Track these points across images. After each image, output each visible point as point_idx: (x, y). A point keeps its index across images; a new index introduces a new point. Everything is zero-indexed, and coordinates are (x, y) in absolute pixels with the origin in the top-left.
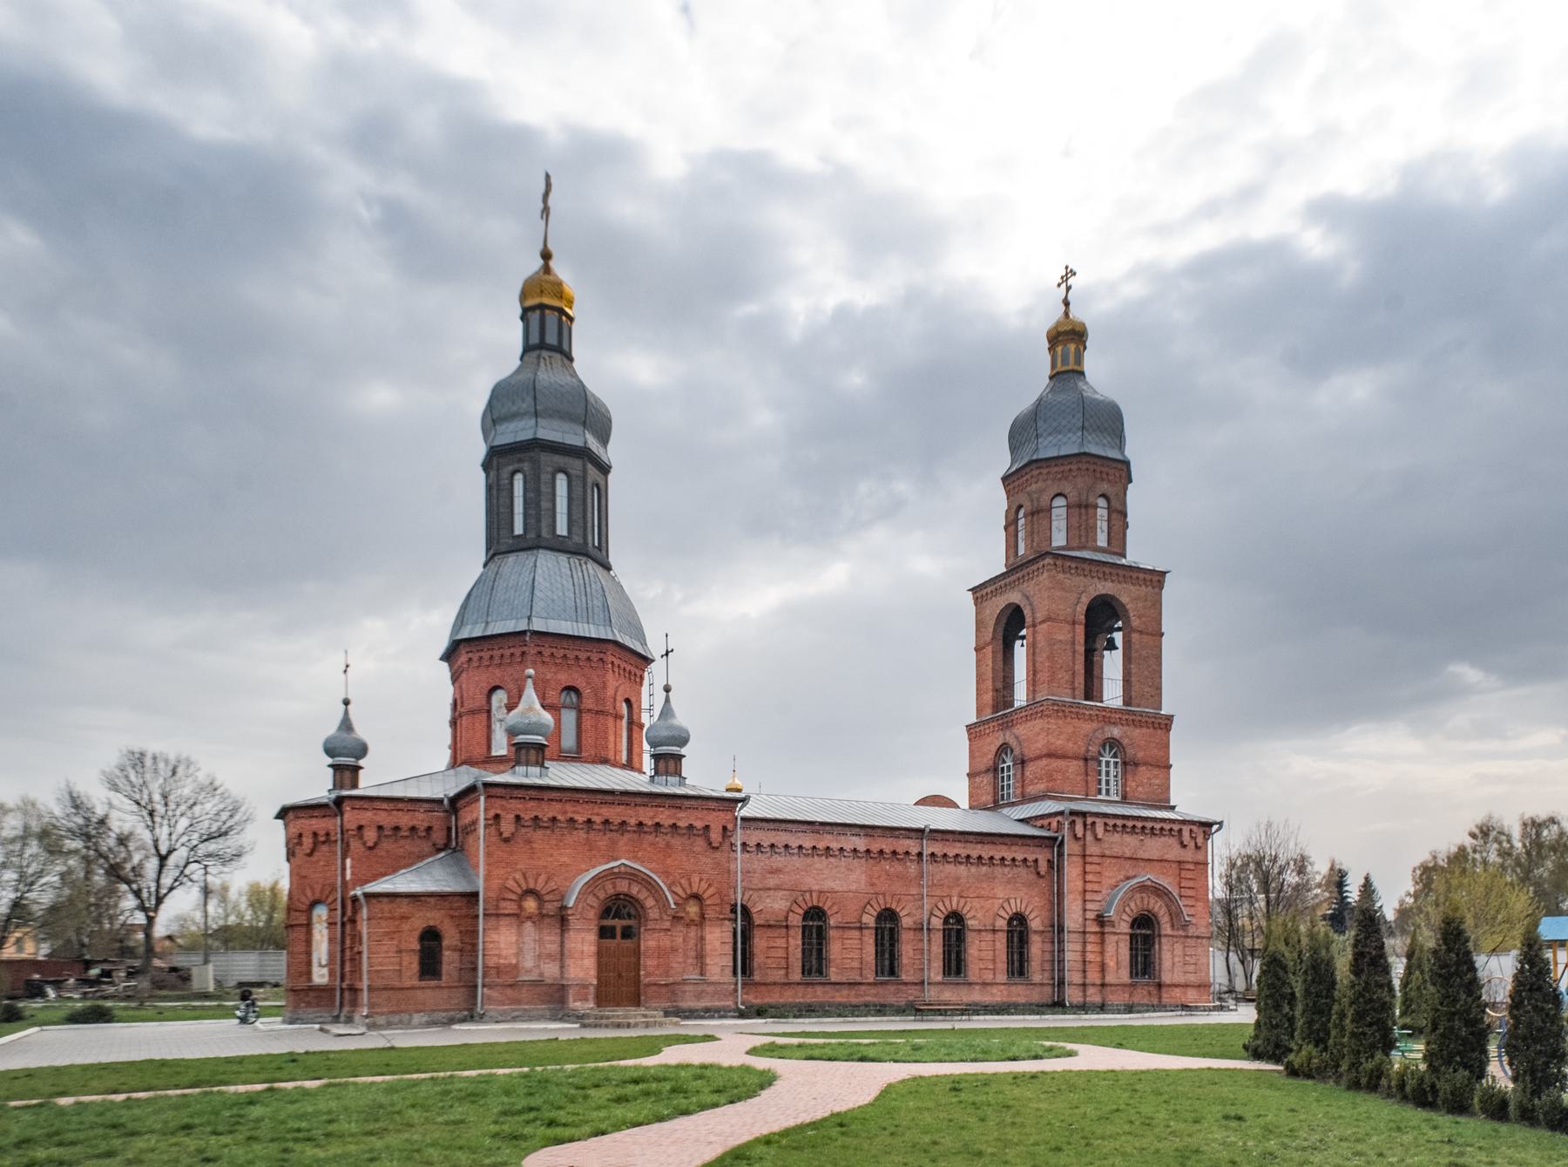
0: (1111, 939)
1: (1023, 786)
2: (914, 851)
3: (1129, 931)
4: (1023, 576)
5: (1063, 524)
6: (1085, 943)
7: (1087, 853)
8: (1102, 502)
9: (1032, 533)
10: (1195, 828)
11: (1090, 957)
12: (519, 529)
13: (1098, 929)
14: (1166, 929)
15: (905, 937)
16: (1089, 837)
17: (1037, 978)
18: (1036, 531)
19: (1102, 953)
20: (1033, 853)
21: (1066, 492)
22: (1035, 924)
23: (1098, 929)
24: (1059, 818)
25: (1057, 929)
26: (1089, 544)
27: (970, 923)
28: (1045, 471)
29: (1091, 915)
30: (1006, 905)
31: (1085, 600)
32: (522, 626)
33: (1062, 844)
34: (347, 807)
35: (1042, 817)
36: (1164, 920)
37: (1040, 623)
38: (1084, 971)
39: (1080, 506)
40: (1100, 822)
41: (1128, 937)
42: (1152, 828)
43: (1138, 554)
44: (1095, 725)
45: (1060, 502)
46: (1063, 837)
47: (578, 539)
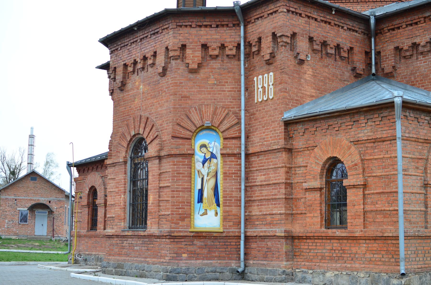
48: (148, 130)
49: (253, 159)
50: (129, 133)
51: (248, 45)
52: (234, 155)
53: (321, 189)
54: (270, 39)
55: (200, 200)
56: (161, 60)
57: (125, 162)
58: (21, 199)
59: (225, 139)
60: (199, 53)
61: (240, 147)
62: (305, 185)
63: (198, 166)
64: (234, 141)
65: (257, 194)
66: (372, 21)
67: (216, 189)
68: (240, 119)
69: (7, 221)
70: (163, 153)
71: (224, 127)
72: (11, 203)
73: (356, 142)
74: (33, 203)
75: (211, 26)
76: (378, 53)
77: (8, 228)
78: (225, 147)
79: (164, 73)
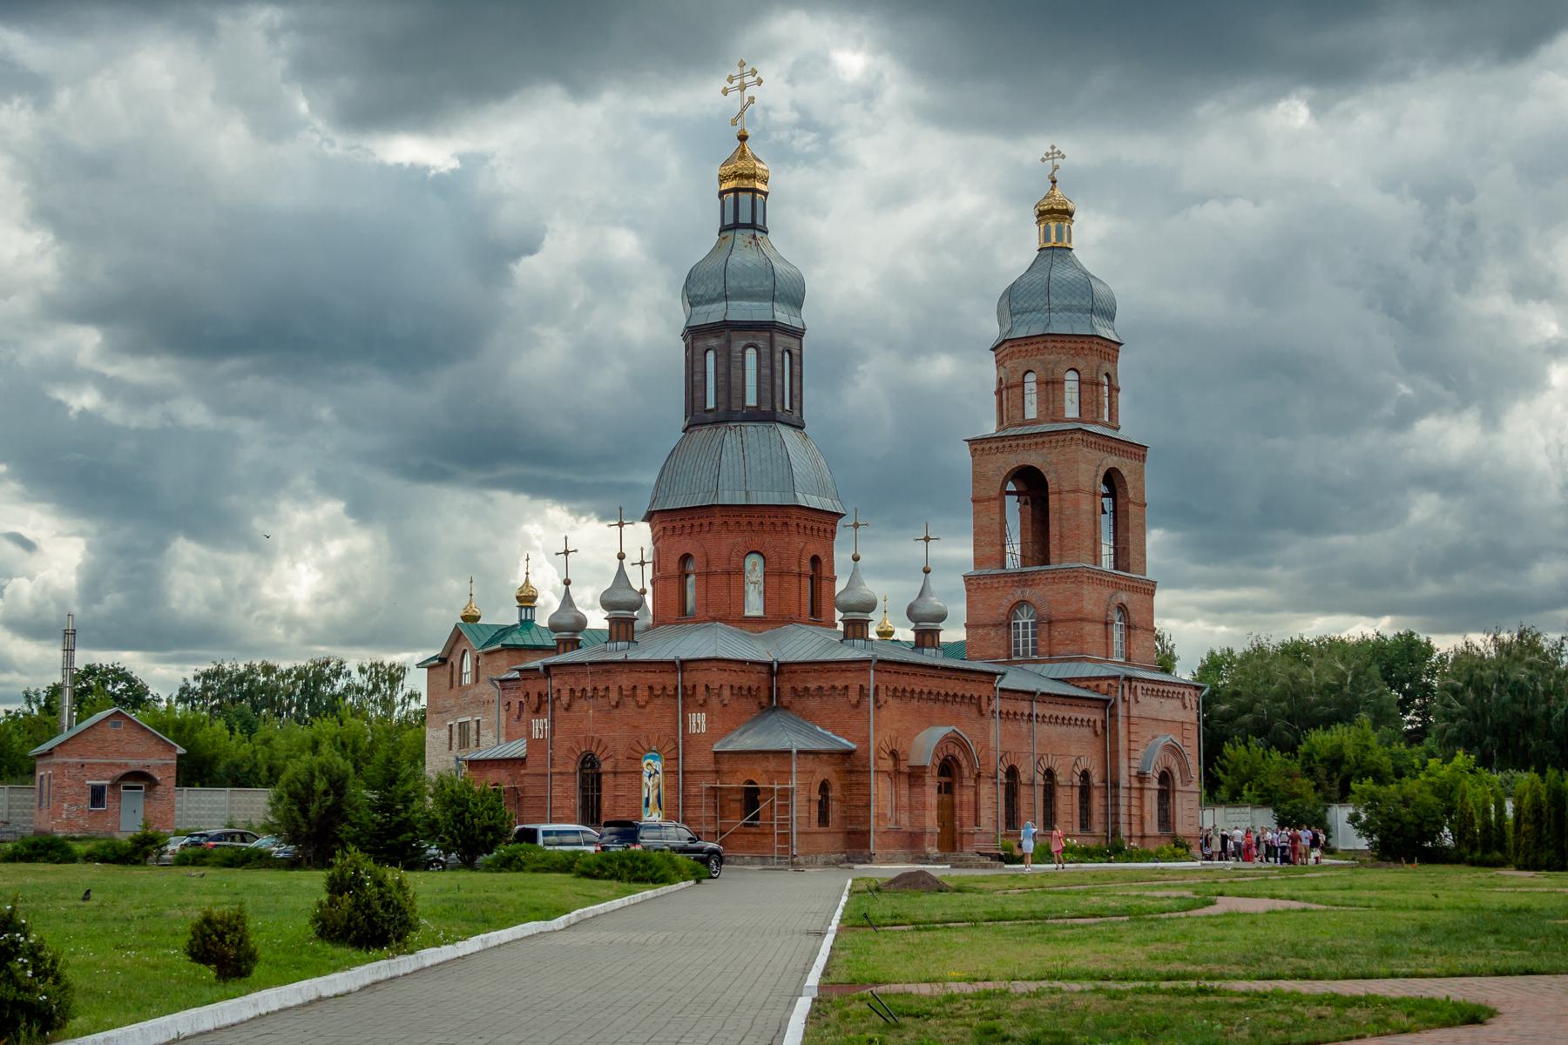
0: (1147, 794)
1: (1050, 644)
2: (1027, 712)
3: (1158, 787)
4: (1043, 442)
5: (1075, 397)
6: (1130, 798)
7: (1132, 714)
8: (1105, 380)
9: (1048, 401)
10: (1192, 692)
11: (1134, 811)
12: (751, 400)
13: (1138, 785)
14: (1179, 786)
15: (1023, 791)
16: (1132, 700)
17: (1098, 829)
18: (1051, 399)
19: (1141, 807)
20: (1094, 714)
22: (1096, 780)
23: (1138, 785)
24: (1110, 682)
26: (1100, 420)
27: (1059, 779)
28: (1059, 345)
29: (1134, 772)
30: (1078, 762)
31: (1102, 473)
32: (788, 500)
33: (1114, 706)
34: (553, 671)
35: (1088, 679)
36: (1177, 776)
37: (1067, 492)
38: (1130, 824)
39: (1092, 384)
40: (1139, 685)
42: (1169, 692)
43: (1129, 428)
45: (1071, 376)
46: (1115, 699)
47: (766, 408)
48: (601, 749)
49: (687, 775)
50: (579, 749)
51: (684, 688)
52: (673, 772)
53: (740, 800)
54: (703, 688)
55: (647, 805)
56: (614, 696)
57: (575, 773)
58: (92, 764)
59: (666, 759)
60: (647, 693)
61: (678, 766)
62: (730, 797)
63: (645, 779)
64: (673, 762)
65: (691, 802)
66: (775, 666)
67: (659, 794)
68: (677, 744)
69: (65, 805)
70: (619, 770)
71: (666, 751)
72: (73, 771)
73: (766, 772)
74: (123, 771)
75: (655, 672)
76: (778, 689)
77: (68, 818)
79: (617, 705)
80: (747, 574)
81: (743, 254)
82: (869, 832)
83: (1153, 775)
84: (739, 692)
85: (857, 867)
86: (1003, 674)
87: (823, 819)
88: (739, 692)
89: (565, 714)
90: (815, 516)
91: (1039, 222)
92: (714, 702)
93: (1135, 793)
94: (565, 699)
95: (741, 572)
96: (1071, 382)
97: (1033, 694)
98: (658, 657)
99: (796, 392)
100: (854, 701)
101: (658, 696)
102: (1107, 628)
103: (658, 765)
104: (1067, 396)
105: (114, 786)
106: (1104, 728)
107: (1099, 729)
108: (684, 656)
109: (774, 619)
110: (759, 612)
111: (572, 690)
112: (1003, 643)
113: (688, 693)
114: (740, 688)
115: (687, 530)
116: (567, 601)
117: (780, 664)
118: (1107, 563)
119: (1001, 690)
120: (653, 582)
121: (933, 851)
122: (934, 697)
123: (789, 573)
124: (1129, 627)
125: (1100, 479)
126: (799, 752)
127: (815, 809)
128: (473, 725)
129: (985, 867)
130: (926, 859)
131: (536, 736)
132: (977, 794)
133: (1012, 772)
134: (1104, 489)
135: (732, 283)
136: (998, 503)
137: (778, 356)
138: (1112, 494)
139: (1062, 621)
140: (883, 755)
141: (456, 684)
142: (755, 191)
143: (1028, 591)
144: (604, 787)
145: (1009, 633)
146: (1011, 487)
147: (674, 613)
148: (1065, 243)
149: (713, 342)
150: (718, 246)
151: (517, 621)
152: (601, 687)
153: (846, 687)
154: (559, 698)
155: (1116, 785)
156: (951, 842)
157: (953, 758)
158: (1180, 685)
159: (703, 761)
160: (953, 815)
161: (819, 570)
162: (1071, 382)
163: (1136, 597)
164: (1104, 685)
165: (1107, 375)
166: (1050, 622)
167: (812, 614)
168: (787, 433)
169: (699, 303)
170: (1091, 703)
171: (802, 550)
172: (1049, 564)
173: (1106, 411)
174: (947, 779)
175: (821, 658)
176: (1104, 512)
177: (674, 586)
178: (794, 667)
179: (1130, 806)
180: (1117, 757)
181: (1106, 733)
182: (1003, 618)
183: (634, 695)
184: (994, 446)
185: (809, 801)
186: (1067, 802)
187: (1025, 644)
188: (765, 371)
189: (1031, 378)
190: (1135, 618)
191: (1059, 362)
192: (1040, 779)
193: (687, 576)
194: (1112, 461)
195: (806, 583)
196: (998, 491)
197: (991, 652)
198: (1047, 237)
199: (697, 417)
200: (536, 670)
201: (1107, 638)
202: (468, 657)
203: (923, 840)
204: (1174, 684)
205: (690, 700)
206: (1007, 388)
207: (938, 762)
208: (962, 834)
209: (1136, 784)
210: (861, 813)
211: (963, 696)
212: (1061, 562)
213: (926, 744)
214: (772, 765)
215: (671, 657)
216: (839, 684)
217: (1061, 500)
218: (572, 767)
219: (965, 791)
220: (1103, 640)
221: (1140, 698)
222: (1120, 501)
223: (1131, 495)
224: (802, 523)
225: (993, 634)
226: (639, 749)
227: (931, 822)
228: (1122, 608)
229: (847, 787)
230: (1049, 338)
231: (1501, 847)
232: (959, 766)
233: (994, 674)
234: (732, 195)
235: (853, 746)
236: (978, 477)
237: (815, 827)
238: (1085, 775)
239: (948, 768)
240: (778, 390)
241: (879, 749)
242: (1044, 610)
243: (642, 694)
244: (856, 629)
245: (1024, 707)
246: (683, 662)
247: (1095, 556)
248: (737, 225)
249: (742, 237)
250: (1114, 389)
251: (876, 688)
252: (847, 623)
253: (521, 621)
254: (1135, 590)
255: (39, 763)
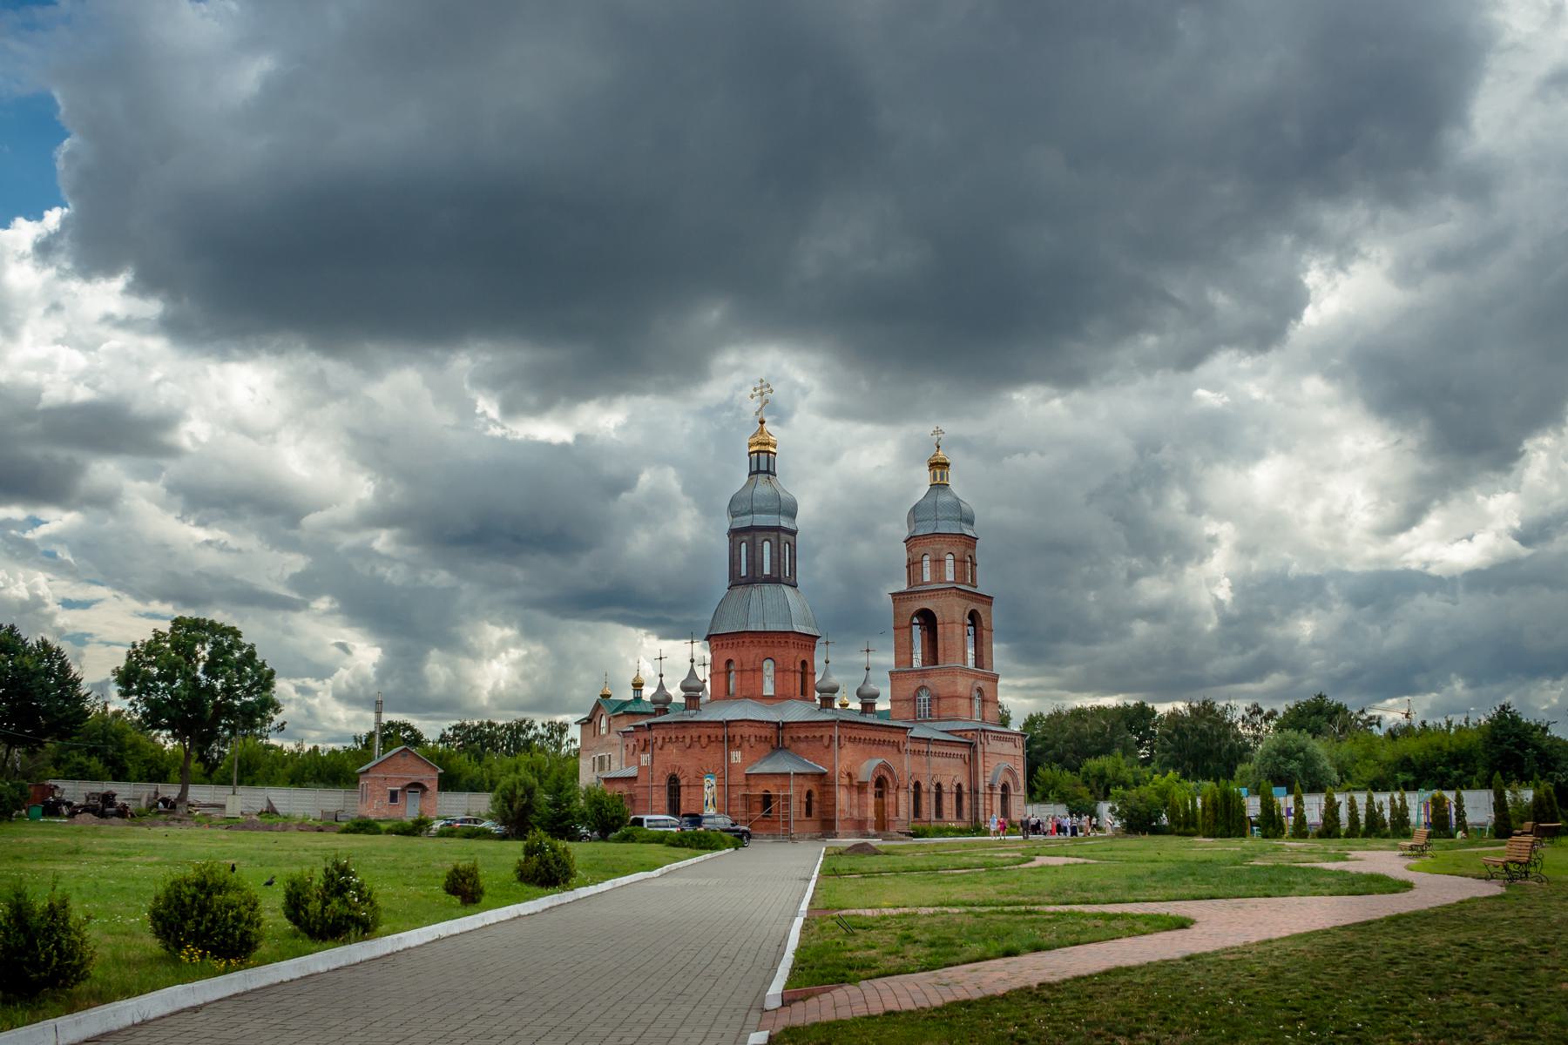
0: (994, 796)
2: (925, 750)
3: (1000, 792)
6: (985, 799)
8: (969, 559)
10: (1020, 737)
11: (987, 807)
12: (767, 571)
14: (1013, 792)
15: (924, 796)
17: (966, 817)
19: (991, 805)
21: (954, 550)
22: (965, 789)
24: (974, 732)
25: (974, 791)
28: (942, 539)
29: (987, 784)
31: (967, 613)
33: (976, 746)
35: (961, 731)
38: (985, 814)
39: (961, 561)
40: (990, 734)
41: (1000, 796)
44: (973, 680)
45: (951, 557)
51: (728, 737)
53: (760, 802)
55: (707, 804)
56: (688, 741)
60: (706, 740)
63: (706, 790)
65: (732, 802)
66: (781, 724)
67: (713, 799)
69: (376, 802)
73: (776, 785)
74: (409, 782)
76: (782, 738)
78: (718, 782)
79: (689, 747)
80: (765, 671)
81: (763, 487)
82: (835, 820)
83: (998, 786)
84: (759, 739)
85: (828, 840)
86: (912, 728)
87: (809, 813)
88: (759, 739)
89: (660, 752)
90: (803, 637)
91: (930, 470)
92: (746, 745)
93: (987, 797)
94: (660, 742)
95: (761, 670)
96: (949, 561)
97: (929, 739)
98: (712, 719)
99: (792, 566)
100: (826, 744)
101: (713, 742)
102: (971, 703)
103: (713, 782)
104: (947, 568)
105: (403, 790)
106: (970, 759)
107: (967, 760)
108: (729, 718)
109: (780, 697)
110: (772, 694)
111: (664, 738)
112: (912, 711)
113: (731, 740)
114: (761, 737)
115: (730, 646)
116: (661, 687)
117: (783, 723)
118: (971, 663)
119: (911, 737)
120: (711, 676)
121: (872, 831)
122: (874, 742)
123: (789, 670)
124: (984, 701)
125: (967, 615)
126: (795, 774)
127: (804, 806)
128: (607, 758)
129: (902, 840)
130: (868, 836)
131: (643, 764)
132: (897, 798)
133: (917, 785)
134: (969, 622)
135: (755, 504)
136: (908, 630)
137: (782, 546)
138: (974, 624)
139: (945, 697)
140: (843, 776)
141: (597, 734)
142: (769, 452)
143: (926, 680)
144: (682, 794)
145: (915, 704)
146: (916, 620)
147: (724, 695)
148: (945, 482)
149: (745, 538)
150: (748, 483)
151: (632, 698)
152: (681, 736)
153: (822, 737)
154: (656, 742)
155: (977, 792)
156: (882, 825)
157: (884, 777)
158: (1013, 734)
159: (741, 779)
160: (883, 809)
161: (805, 669)
162: (949, 561)
163: (987, 683)
164: (970, 734)
165: (970, 556)
166: (939, 698)
167: (802, 694)
168: (788, 590)
169: (737, 516)
170: (963, 745)
171: (796, 657)
172: (936, 663)
173: (969, 577)
174: (880, 789)
175: (806, 720)
176: (969, 635)
177: (722, 679)
178: (792, 725)
179: (985, 804)
180: (977, 776)
181: (971, 762)
182: (911, 696)
183: (699, 741)
184: (906, 597)
185: (801, 802)
186: (949, 803)
187: (925, 710)
188: (775, 555)
189: (926, 558)
190: (987, 695)
191: (942, 549)
192: (933, 789)
193: (730, 672)
194: (973, 606)
195: (799, 676)
196: (908, 622)
197: (905, 715)
198: (935, 479)
199: (736, 581)
200: (643, 726)
201: (971, 707)
202: (604, 718)
203: (866, 826)
204: (1010, 734)
205: (732, 744)
206: (913, 564)
207: (875, 780)
208: (888, 821)
209: (988, 791)
210: (830, 809)
211: (889, 741)
212: (944, 664)
213: (867, 769)
214: (779, 781)
215: (721, 719)
216: (818, 734)
217: (944, 628)
218: (664, 782)
219: (890, 796)
220: (969, 709)
221: (990, 741)
222: (978, 628)
223: (984, 625)
224: (796, 642)
225: (906, 705)
226: (702, 772)
227: (871, 813)
228: (980, 690)
229: (822, 794)
230: (937, 535)
231: (1194, 825)
232: (887, 782)
233: (907, 729)
234: (756, 454)
235: (826, 771)
236: (896, 615)
237: (804, 817)
238: (959, 786)
239: (880, 783)
240: (782, 565)
241: (841, 772)
242: (935, 692)
243: (704, 741)
244: (827, 702)
245: (924, 747)
246: (728, 722)
247: (964, 660)
248: (758, 472)
249: (761, 477)
250: (974, 564)
251: (839, 737)
252: (822, 699)
253: (635, 698)
254: (987, 679)
255: (361, 777)
